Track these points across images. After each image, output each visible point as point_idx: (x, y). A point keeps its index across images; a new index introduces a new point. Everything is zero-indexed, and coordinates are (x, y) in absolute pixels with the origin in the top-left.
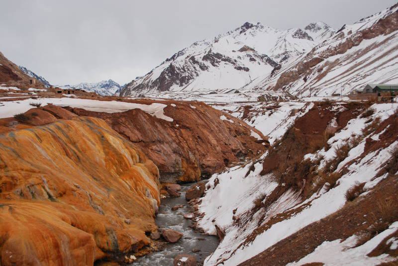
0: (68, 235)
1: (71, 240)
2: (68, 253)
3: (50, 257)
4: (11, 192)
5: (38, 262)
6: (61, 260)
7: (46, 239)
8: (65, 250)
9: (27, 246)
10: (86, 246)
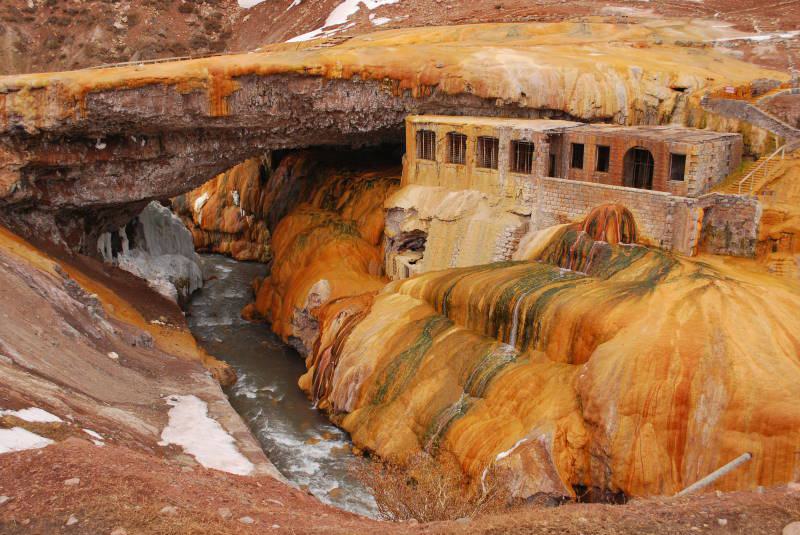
0: (731, 390)
1: (733, 405)
2: (707, 430)
3: (653, 415)
4: (790, 257)
5: (612, 413)
6: (682, 440)
7: (669, 375)
8: (705, 420)
9: (614, 369)
10: (773, 438)
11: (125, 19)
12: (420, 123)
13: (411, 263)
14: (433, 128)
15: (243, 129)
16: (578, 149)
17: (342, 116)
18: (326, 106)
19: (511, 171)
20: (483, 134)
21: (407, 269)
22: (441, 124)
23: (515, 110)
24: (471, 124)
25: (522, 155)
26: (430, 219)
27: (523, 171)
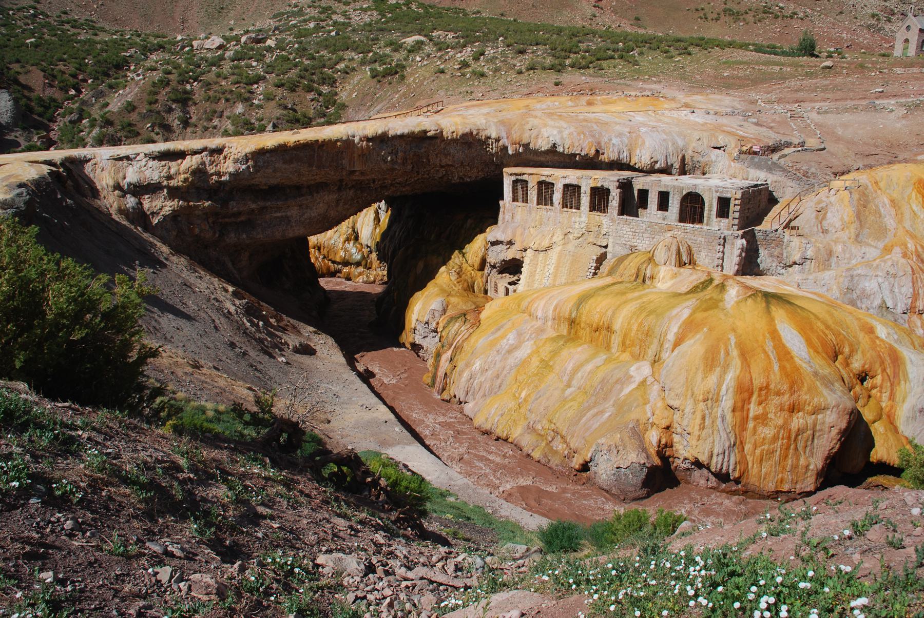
11: (261, 97)
12: (516, 174)
13: (510, 284)
14: (525, 177)
15: (374, 181)
16: (644, 194)
17: (453, 169)
18: (440, 160)
19: (591, 211)
21: (507, 290)
22: (534, 175)
23: (591, 163)
25: (599, 198)
26: (526, 250)
27: (599, 210)
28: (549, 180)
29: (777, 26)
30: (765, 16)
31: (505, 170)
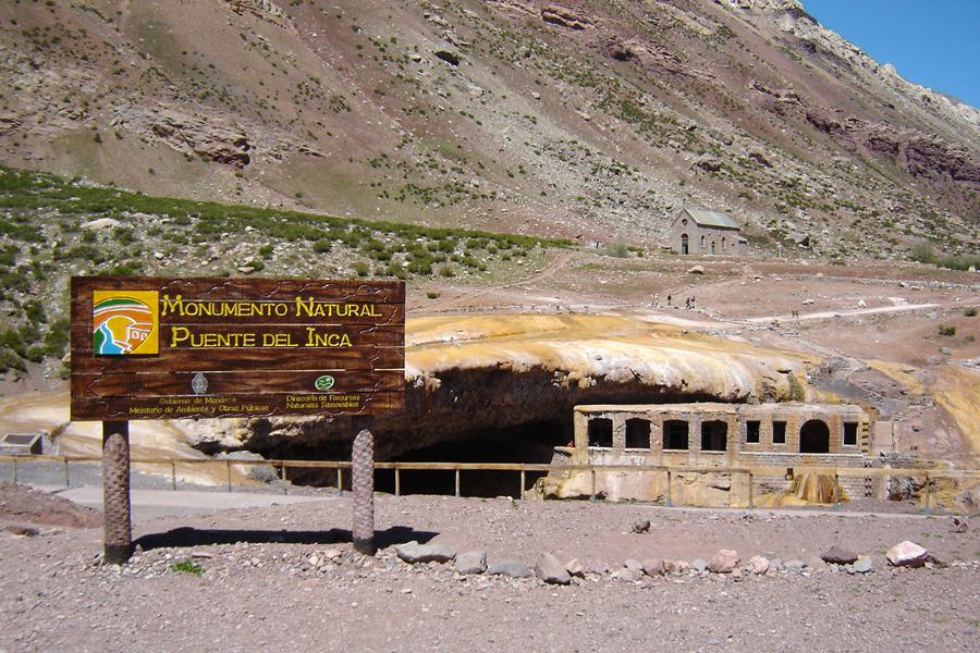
12: (594, 413)
14: (610, 416)
20: (667, 418)
22: (619, 415)
23: (673, 395)
24: (654, 412)
28: (642, 417)
29: (480, 208)
30: (462, 195)
31: (575, 408)
